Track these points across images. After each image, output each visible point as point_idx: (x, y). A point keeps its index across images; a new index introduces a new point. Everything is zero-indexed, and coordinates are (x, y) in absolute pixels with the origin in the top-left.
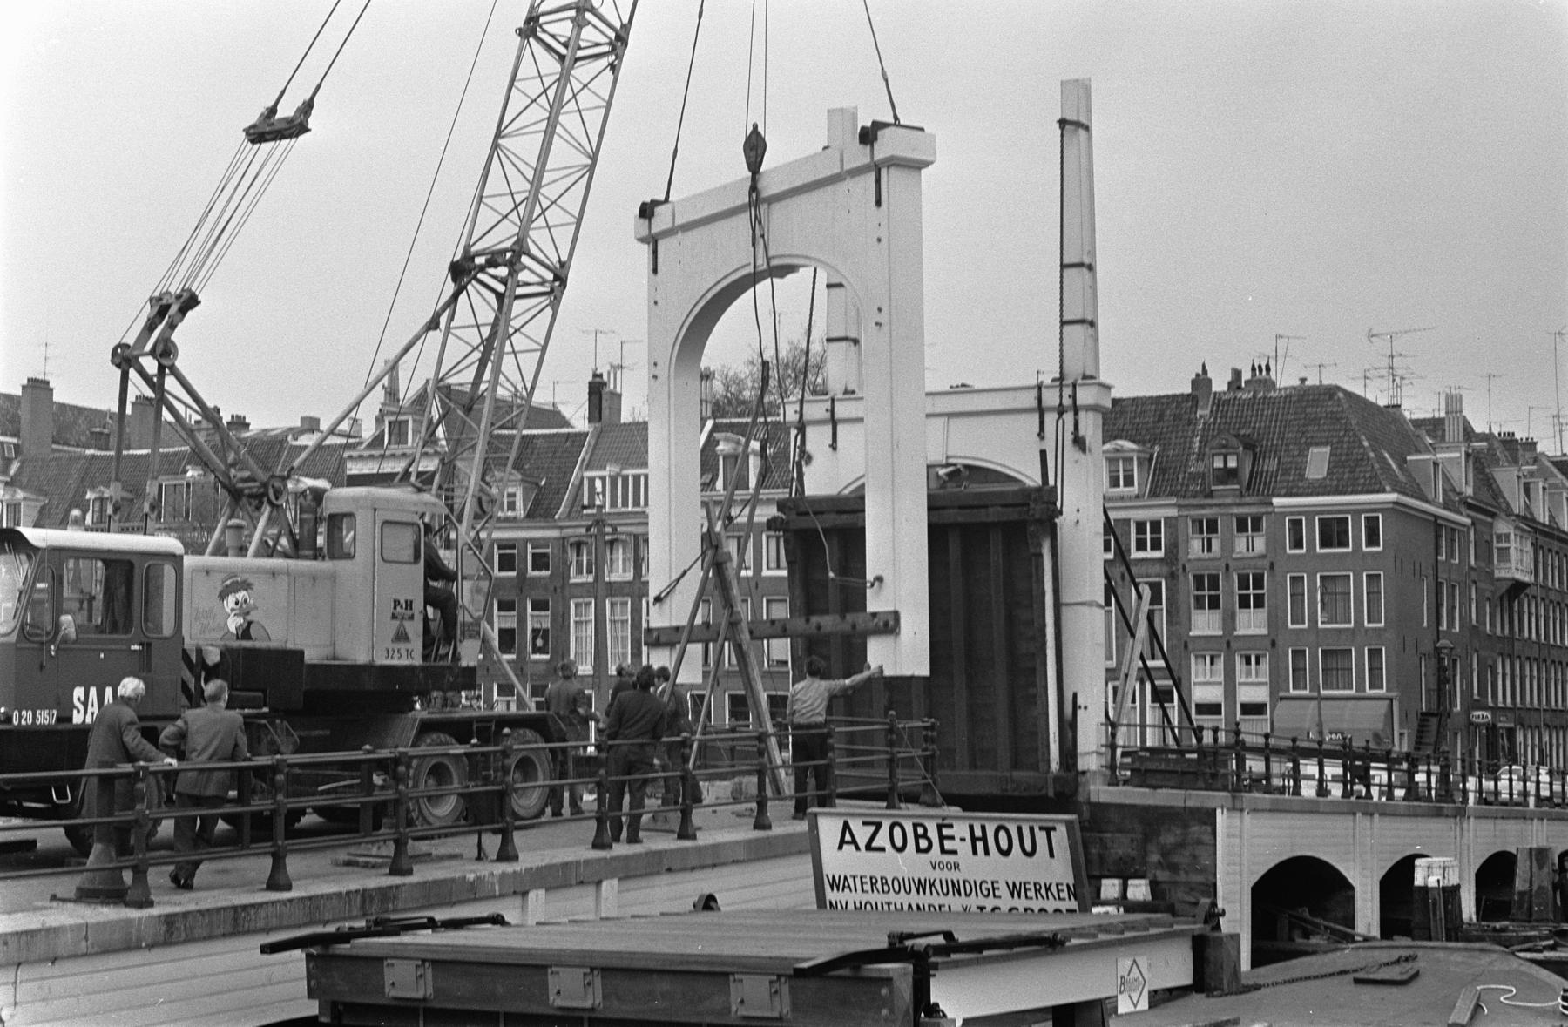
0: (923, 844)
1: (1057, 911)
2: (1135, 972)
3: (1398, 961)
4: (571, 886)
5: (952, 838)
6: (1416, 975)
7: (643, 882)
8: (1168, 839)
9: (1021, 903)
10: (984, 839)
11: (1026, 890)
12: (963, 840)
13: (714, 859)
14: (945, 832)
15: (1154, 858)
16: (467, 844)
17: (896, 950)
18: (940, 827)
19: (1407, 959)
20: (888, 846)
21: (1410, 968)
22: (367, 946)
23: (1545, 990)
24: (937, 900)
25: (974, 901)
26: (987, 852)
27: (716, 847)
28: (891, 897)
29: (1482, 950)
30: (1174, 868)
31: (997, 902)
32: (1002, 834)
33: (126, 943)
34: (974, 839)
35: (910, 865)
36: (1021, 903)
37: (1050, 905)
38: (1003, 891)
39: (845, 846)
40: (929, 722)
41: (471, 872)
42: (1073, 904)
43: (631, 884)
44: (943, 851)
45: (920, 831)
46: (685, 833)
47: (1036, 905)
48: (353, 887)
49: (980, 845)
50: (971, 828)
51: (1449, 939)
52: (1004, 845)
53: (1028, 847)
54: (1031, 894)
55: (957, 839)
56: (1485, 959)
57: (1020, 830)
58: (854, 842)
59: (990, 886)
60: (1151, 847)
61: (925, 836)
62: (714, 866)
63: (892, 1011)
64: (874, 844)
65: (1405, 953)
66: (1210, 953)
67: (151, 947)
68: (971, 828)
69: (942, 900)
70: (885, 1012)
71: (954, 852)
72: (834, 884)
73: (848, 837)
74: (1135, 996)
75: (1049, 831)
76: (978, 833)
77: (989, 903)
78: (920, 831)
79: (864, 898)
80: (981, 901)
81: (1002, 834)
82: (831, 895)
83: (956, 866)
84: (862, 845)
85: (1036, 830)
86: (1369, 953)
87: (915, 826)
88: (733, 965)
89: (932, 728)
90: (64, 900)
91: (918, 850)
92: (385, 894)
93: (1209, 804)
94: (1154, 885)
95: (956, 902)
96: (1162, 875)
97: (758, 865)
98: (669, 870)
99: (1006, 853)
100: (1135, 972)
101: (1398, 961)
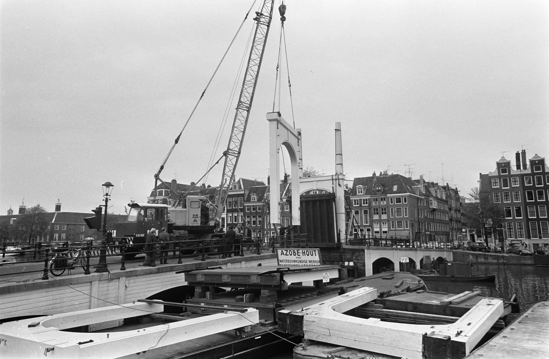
1: (317, 265)
2: (326, 275)
3: (390, 275)
4: (236, 263)
5: (299, 253)
6: (393, 278)
7: (249, 262)
8: (356, 255)
9: (311, 264)
10: (304, 253)
13: (264, 258)
15: (354, 258)
16: (218, 256)
17: (278, 271)
19: (392, 275)
20: (289, 254)
21: (392, 276)
22: (194, 272)
23: (415, 279)
24: (297, 264)
25: (303, 264)
26: (305, 255)
27: (264, 256)
29: (406, 273)
30: (358, 260)
31: (307, 264)
32: (307, 252)
33: (151, 273)
34: (303, 253)
35: (293, 258)
36: (311, 264)
37: (316, 264)
38: (308, 262)
40: (307, 234)
41: (216, 260)
42: (319, 264)
43: (248, 262)
46: (259, 253)
47: (313, 264)
48: (193, 263)
49: (304, 254)
51: (407, 271)
52: (308, 254)
53: (312, 254)
56: (406, 275)
57: (310, 251)
60: (354, 256)
62: (264, 259)
63: (276, 281)
65: (392, 274)
66: (341, 272)
67: (155, 273)
69: (298, 264)
70: (275, 281)
71: (300, 255)
72: (280, 261)
74: (326, 280)
75: (315, 251)
76: (303, 252)
77: (306, 264)
80: (305, 264)
81: (307, 252)
82: (280, 263)
83: (300, 258)
86: (386, 274)
88: (251, 274)
89: (307, 235)
90: (141, 266)
92: (200, 264)
93: (363, 248)
94: (354, 263)
95: (300, 264)
96: (356, 261)
97: (272, 259)
98: (255, 260)
99: (308, 255)
100: (326, 275)
101: (390, 275)
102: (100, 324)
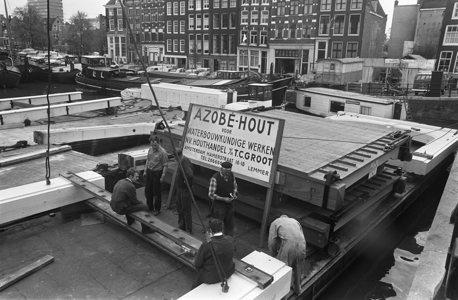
0: (222, 121)
5: (233, 120)
10: (245, 123)
11: (255, 146)
12: (237, 121)
14: (232, 117)
18: (231, 115)
28: (206, 139)
34: (241, 122)
38: (246, 146)
39: (196, 118)
44: (229, 125)
45: (223, 116)
49: (242, 125)
50: (241, 117)
52: (252, 127)
54: (256, 148)
55: (235, 121)
57: (260, 120)
58: (200, 117)
59: (242, 142)
61: (224, 118)
64: (206, 119)
68: (241, 117)
71: (232, 126)
73: (199, 115)
75: (271, 123)
76: (243, 120)
78: (223, 116)
79: (197, 138)
84: (202, 118)
85: (266, 122)
87: (222, 113)
91: (220, 124)
99: (251, 130)
102: (10, 157)
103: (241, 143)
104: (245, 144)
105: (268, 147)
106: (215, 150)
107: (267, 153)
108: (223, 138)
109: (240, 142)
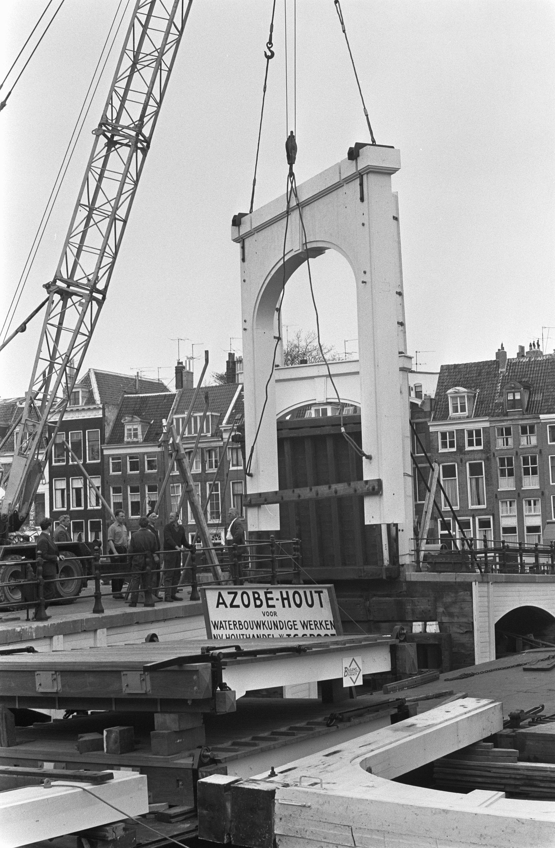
5: (272, 599)
10: (288, 599)
11: (310, 625)
12: (277, 599)
14: (269, 596)
18: (266, 593)
28: (244, 631)
34: (283, 599)
38: (299, 626)
39: (220, 606)
44: (269, 606)
45: (256, 596)
50: (281, 593)
52: (298, 602)
54: (313, 627)
57: (305, 592)
59: (292, 623)
61: (259, 598)
64: (234, 604)
68: (281, 593)
71: (273, 606)
73: (221, 601)
75: (319, 593)
76: (285, 596)
78: (256, 596)
84: (228, 604)
85: (313, 592)
87: (254, 593)
91: (256, 606)
103: (291, 625)
104: (296, 625)
105: (325, 621)
106: (278, 629)
107: (327, 629)
108: (266, 623)
109: (289, 623)
